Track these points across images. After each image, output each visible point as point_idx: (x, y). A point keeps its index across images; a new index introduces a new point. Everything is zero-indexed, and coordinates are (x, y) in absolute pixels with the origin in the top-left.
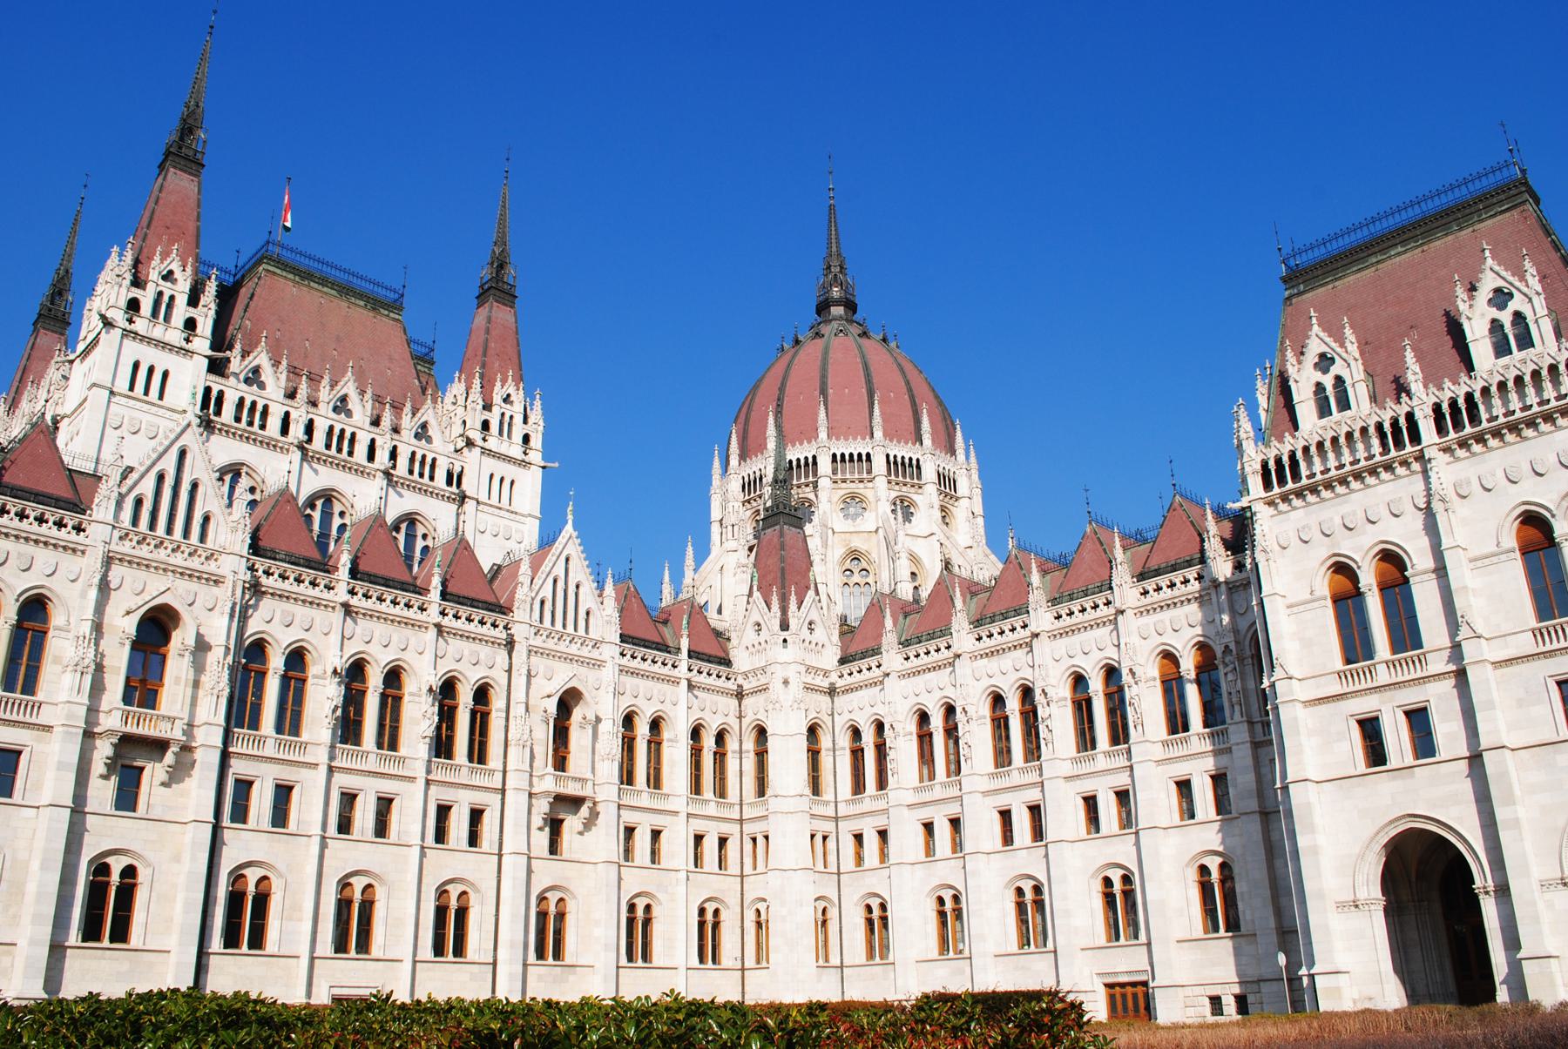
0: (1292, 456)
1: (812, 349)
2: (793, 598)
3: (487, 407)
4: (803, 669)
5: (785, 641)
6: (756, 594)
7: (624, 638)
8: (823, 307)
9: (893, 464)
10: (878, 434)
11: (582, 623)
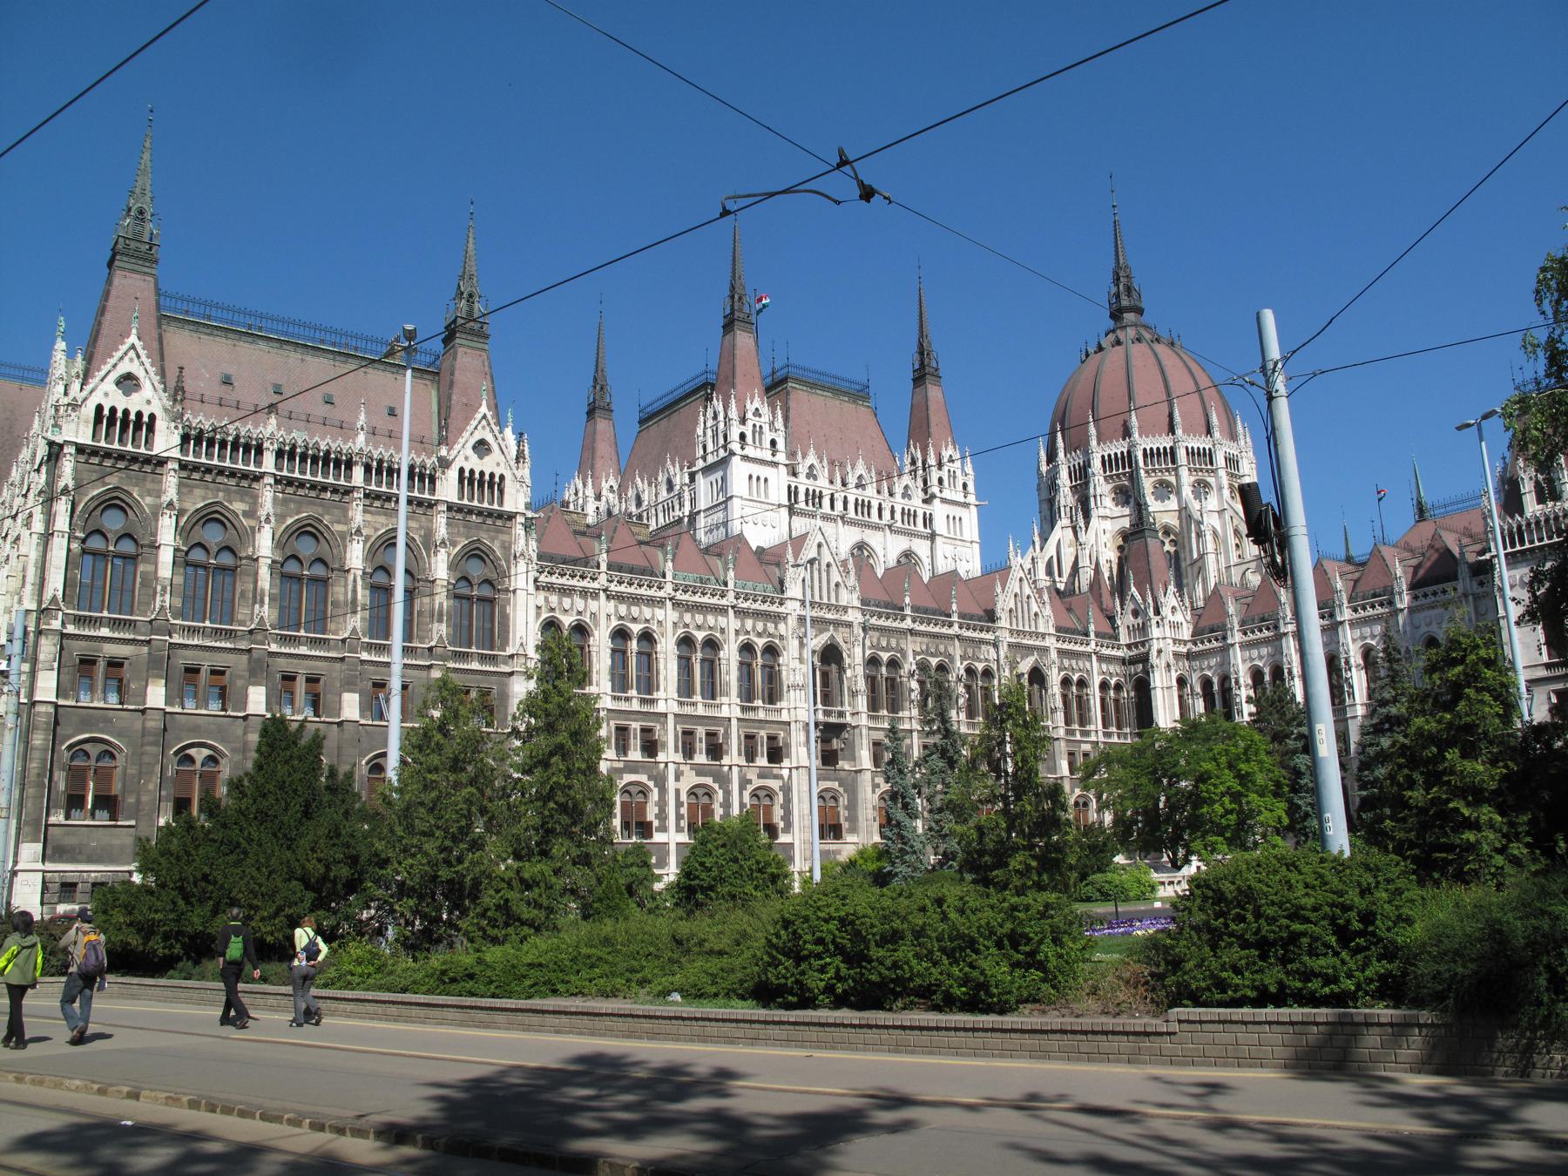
0: (1519, 527)
1: (1114, 356)
3: (940, 465)
6: (1133, 589)
7: (1058, 629)
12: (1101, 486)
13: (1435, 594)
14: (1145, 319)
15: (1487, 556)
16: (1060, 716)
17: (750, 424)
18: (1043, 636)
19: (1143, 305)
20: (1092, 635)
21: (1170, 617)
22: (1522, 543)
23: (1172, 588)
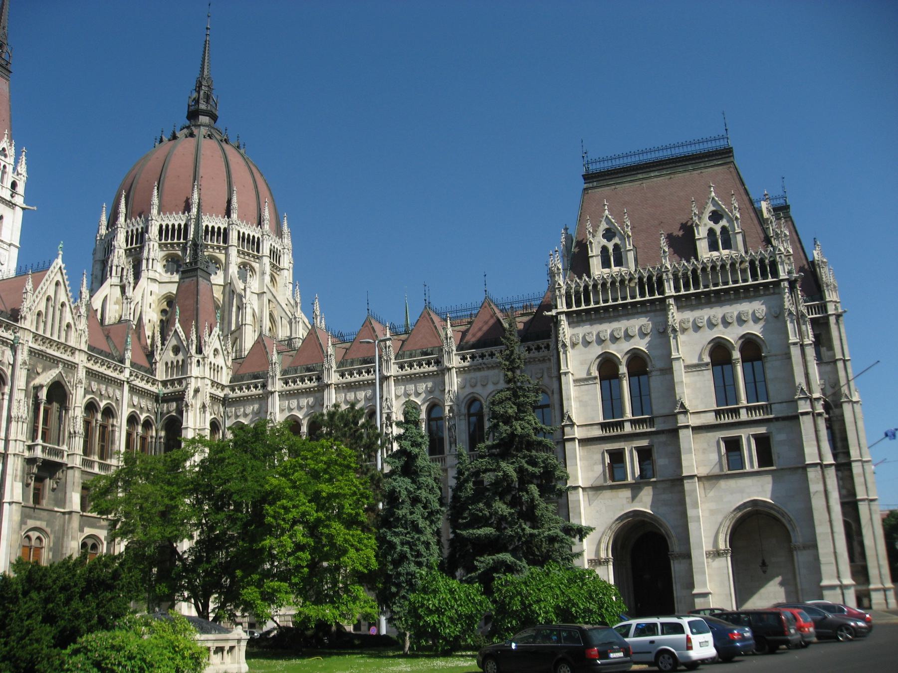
1: (185, 146)
4: (209, 383)
5: (198, 361)
6: (177, 325)
7: (91, 348)
8: (193, 115)
11: (63, 334)
12: (154, 251)
13: (482, 356)
14: (219, 124)
15: (554, 312)
16: (78, 443)
18: (73, 350)
19: (217, 113)
20: (128, 363)
21: (211, 358)
22: (587, 302)
23: (216, 330)
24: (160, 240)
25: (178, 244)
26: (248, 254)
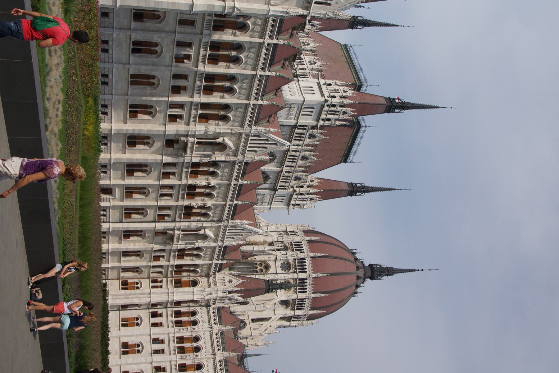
2: (240, 295)
6: (241, 281)
7: (225, 247)
9: (302, 301)
10: (313, 295)
11: (230, 236)
17: (339, 109)
24: (298, 260)
25: (296, 269)
26: (295, 305)
